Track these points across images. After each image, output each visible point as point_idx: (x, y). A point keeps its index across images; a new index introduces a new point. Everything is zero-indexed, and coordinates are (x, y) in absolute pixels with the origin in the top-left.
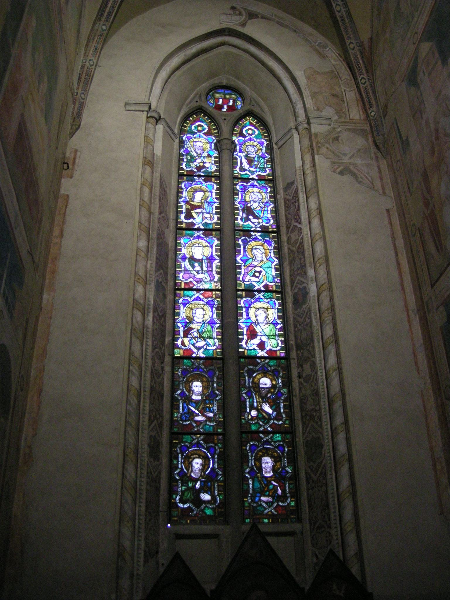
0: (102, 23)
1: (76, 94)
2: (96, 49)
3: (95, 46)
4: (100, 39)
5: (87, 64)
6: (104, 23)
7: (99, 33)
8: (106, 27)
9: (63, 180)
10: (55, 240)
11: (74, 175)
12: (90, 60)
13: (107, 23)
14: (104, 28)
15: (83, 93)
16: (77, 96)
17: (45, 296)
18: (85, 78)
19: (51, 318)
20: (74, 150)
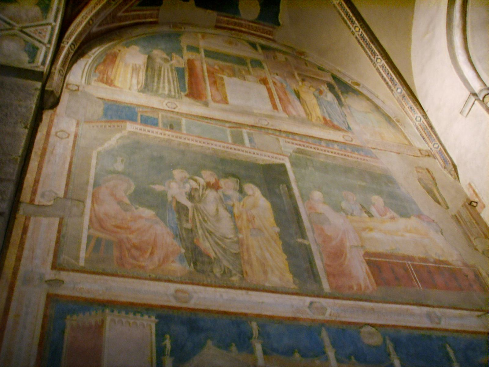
0: (395, 90)
1: (431, 151)
2: (411, 108)
3: (408, 108)
4: (406, 99)
5: (417, 123)
6: (396, 88)
7: (401, 98)
8: (400, 88)
9: (482, 215)
11: (484, 203)
12: (416, 119)
13: (397, 86)
14: (399, 90)
15: (434, 144)
16: (433, 151)
18: (425, 133)
20: (468, 186)
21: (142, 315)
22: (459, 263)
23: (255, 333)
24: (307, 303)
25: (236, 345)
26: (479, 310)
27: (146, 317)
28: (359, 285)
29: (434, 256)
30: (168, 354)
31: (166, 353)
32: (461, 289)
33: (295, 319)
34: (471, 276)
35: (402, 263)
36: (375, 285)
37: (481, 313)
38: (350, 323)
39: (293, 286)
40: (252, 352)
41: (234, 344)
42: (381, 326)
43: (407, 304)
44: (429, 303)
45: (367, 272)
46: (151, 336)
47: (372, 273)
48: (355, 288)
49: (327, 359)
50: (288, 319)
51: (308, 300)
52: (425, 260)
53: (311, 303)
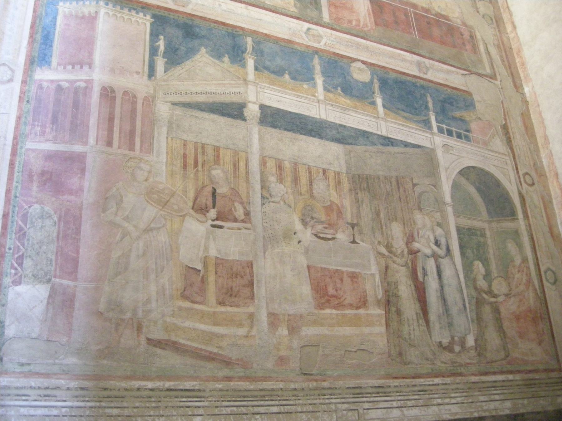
10: (512, 36)
17: (526, 90)
19: (539, 105)
21: (137, 13)
22: (459, 21)
23: (249, 48)
24: (305, 29)
25: (229, 58)
26: (465, 70)
27: (141, 15)
28: (358, 21)
29: (436, 9)
30: (160, 55)
31: (159, 53)
32: (455, 47)
33: (290, 42)
34: (466, 36)
35: (404, 9)
36: (374, 24)
37: (467, 73)
38: (342, 56)
39: (293, 10)
40: (244, 65)
41: (226, 55)
42: (372, 64)
43: (401, 49)
44: (421, 52)
45: (368, 10)
46: (145, 34)
47: (373, 11)
48: (354, 23)
49: (315, 86)
50: (283, 40)
51: (306, 25)
52: (427, 11)
53: (309, 29)
